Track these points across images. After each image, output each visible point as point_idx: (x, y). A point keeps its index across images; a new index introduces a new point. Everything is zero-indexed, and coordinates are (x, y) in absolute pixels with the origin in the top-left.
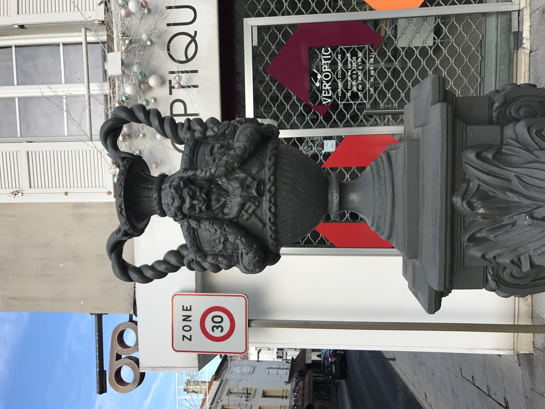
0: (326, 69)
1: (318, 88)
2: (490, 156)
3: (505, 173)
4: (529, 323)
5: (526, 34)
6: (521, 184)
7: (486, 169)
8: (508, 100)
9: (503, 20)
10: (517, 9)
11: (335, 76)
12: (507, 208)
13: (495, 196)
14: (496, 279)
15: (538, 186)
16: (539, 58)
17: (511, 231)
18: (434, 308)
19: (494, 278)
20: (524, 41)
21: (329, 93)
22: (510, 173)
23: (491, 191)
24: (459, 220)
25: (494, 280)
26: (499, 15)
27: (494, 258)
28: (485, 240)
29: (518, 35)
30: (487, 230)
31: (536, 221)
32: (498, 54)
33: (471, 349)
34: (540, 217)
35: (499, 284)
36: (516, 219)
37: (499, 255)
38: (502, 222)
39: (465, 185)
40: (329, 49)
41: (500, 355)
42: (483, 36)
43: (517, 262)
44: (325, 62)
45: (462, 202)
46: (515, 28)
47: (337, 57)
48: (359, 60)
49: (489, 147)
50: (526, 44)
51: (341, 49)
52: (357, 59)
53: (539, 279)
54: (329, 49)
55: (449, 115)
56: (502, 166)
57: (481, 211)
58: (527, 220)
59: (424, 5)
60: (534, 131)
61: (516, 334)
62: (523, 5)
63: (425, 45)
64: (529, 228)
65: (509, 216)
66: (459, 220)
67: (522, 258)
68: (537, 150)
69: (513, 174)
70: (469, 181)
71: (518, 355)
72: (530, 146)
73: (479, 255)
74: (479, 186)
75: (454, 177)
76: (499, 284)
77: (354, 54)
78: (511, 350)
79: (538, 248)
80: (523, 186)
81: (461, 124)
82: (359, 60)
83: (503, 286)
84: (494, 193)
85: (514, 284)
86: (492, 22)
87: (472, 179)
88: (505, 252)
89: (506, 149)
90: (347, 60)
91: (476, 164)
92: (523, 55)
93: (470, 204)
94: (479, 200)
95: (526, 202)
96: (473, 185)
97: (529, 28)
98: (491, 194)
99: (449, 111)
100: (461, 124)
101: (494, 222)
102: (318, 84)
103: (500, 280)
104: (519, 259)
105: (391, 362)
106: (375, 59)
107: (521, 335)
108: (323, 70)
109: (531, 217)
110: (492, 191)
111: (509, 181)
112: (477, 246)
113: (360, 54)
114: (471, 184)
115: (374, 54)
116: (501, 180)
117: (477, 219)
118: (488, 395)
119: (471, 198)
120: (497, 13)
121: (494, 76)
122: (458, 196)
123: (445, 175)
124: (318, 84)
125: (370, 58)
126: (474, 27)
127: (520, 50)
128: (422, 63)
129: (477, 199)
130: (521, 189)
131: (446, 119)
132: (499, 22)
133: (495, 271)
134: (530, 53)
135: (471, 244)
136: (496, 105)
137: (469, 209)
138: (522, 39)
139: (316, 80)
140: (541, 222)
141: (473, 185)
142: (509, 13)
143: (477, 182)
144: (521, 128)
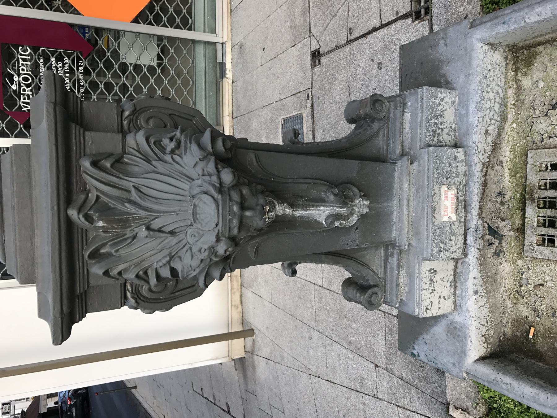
0: (25, 70)
1: (15, 91)
2: (108, 165)
3: (124, 183)
4: (241, 329)
5: (228, 66)
6: (137, 195)
8: (138, 109)
9: (210, 49)
10: (221, 41)
11: (37, 80)
14: (136, 296)
16: (239, 89)
17: (133, 244)
18: (61, 338)
19: (133, 295)
20: (227, 72)
21: (29, 99)
22: (128, 183)
25: (133, 297)
26: (206, 45)
27: (120, 273)
28: (109, 255)
30: (111, 245)
31: (151, 233)
33: (192, 364)
34: (156, 229)
35: (139, 301)
37: (126, 270)
39: (83, 197)
40: (28, 48)
41: (221, 364)
42: (193, 62)
43: (144, 276)
44: (24, 63)
45: (78, 214)
46: (219, 59)
47: (39, 59)
48: (67, 67)
49: (110, 155)
50: (229, 74)
51: (43, 51)
52: (64, 65)
53: (178, 291)
54: (28, 48)
55: (58, 117)
56: (121, 175)
58: (143, 232)
60: (152, 142)
61: (230, 341)
62: (225, 39)
63: (139, 62)
64: (148, 240)
67: (149, 272)
68: (156, 160)
69: (132, 184)
70: (89, 191)
71: (234, 360)
72: (150, 157)
73: (101, 272)
74: (98, 197)
75: (68, 187)
76: (139, 301)
77: (60, 59)
78: (226, 357)
79: (160, 260)
80: (139, 197)
82: (67, 67)
86: (200, 50)
87: (91, 189)
88: (131, 266)
90: (51, 64)
91: (93, 173)
92: (227, 84)
93: (88, 218)
95: (142, 213)
96: (92, 197)
97: (230, 61)
98: (112, 206)
99: (58, 113)
101: (116, 235)
102: (14, 87)
103: (140, 296)
104: (146, 273)
105: (133, 391)
106: (85, 69)
107: (235, 341)
108: (21, 72)
109: (148, 228)
110: (112, 203)
111: (129, 191)
113: (67, 60)
114: (90, 195)
115: (85, 63)
116: (120, 191)
117: (98, 233)
118: (215, 404)
121: (204, 100)
122: (73, 208)
123: (55, 185)
124: (14, 87)
127: (225, 79)
130: (139, 200)
131: (53, 121)
132: (207, 51)
133: (134, 288)
134: (233, 83)
135: (94, 261)
136: (127, 113)
137: (87, 223)
138: (225, 70)
139: (12, 81)
140: (157, 233)
141: (92, 197)
142: (214, 44)
143: (96, 193)
144: (141, 137)
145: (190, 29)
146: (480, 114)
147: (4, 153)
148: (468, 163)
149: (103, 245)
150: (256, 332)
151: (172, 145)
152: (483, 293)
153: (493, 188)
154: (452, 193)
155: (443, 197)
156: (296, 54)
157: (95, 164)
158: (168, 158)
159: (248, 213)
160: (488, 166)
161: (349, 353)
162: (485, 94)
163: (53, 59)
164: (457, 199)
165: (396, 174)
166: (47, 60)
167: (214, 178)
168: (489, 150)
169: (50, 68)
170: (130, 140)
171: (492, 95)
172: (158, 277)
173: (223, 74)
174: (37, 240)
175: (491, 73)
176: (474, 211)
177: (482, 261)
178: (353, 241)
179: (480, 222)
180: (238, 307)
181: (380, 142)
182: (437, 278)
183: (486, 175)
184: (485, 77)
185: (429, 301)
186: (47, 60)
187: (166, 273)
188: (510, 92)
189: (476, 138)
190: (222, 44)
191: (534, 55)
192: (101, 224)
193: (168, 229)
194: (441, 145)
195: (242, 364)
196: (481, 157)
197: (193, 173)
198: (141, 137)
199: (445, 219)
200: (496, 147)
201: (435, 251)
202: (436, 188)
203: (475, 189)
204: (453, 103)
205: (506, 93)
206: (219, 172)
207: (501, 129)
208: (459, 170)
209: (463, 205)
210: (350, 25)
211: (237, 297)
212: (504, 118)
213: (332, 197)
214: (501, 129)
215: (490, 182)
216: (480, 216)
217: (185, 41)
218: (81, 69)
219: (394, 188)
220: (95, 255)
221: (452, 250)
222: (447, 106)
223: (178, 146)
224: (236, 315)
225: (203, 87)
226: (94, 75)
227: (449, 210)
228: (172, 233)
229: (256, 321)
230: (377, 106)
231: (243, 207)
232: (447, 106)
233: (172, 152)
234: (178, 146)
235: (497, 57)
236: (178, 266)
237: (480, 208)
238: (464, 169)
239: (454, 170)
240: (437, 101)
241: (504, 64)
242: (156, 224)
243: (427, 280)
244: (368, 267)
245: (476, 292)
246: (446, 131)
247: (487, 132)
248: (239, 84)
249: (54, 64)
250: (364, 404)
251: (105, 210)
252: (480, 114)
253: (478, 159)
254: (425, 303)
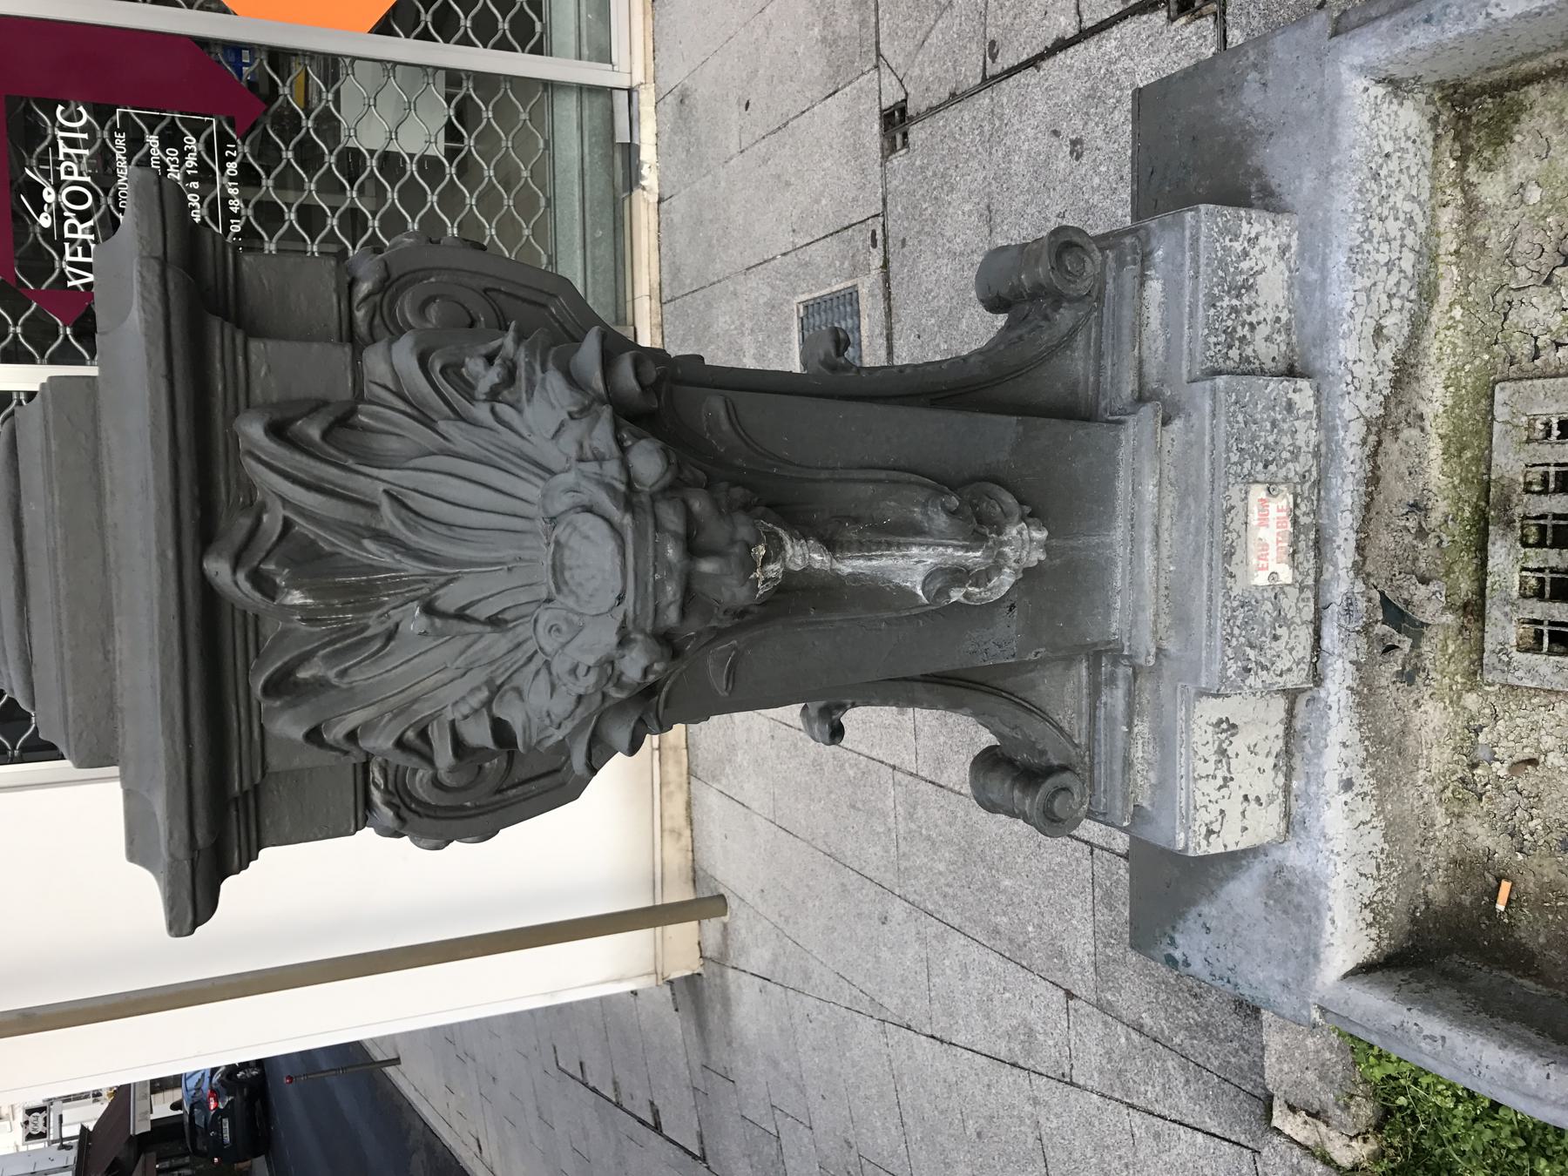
1: (47, 233)
2: (315, 433)
3: (359, 484)
4: (688, 895)
5: (648, 154)
6: (398, 517)
7: (305, 472)
8: (395, 275)
9: (595, 105)
10: (626, 85)
11: (110, 201)
12: (366, 592)
13: (332, 554)
14: (396, 801)
15: (446, 520)
16: (677, 218)
17: (387, 654)
18: (190, 917)
19: (388, 797)
20: (645, 171)
21: (87, 253)
22: (373, 483)
23: (325, 540)
24: (239, 634)
25: (389, 804)
26: (585, 95)
27: (352, 736)
28: (320, 685)
29: (630, 151)
30: (325, 657)
31: (438, 622)
32: (587, 195)
33: (552, 993)
34: (452, 610)
35: (405, 813)
36: (396, 619)
37: (368, 726)
38: (363, 630)
39: (246, 522)
40: (81, 109)
41: (634, 993)
42: (546, 143)
43: (418, 743)
44: (72, 151)
45: (234, 571)
46: (622, 136)
47: (113, 139)
48: (191, 161)
49: (315, 407)
51: (124, 116)
52: (183, 155)
53: (514, 786)
54: (81, 109)
55: (172, 298)
56: (350, 462)
57: (296, 598)
58: (414, 621)
59: (383, 28)
60: (438, 367)
61: (659, 929)
62: (638, 78)
63: (394, 147)
64: (429, 643)
65: (380, 612)
66: (239, 634)
67: (434, 732)
68: (448, 418)
69: (381, 487)
70: (263, 508)
71: (671, 982)
72: (432, 408)
73: (298, 733)
74: (287, 524)
75: (204, 496)
76: (405, 813)
77: (171, 139)
78: (649, 974)
79: (463, 698)
80: (404, 522)
81: (227, 332)
82: (191, 161)
83: (416, 818)
84: (333, 544)
85: (445, 808)
86: (567, 110)
87: (269, 504)
88: (382, 716)
89: (367, 414)
90: (148, 155)
91: (274, 456)
92: (643, 205)
93: (260, 581)
94: (285, 567)
95: (412, 567)
96: (272, 523)
97: (653, 139)
98: (327, 548)
99: (171, 286)
100: (227, 332)
101: (341, 629)
102: (45, 221)
103: (407, 800)
104: (423, 734)
105: (390, 1070)
106: (244, 167)
107: (672, 930)
108: (63, 177)
109: (429, 610)
110: (328, 540)
111: (373, 507)
112: (295, 706)
113: (191, 142)
114: (265, 518)
115: (242, 150)
116: (350, 507)
117: (292, 626)
118: (618, 1105)
119: (262, 561)
120: (581, 88)
121: (579, 253)
122: (219, 555)
123: (167, 489)
124: (45, 221)
125: (223, 161)
126: (524, 116)
127: (637, 193)
128: (389, 195)
129: (277, 564)
130: (402, 532)
131: (160, 308)
132: (586, 113)
133: (391, 777)
134: (660, 201)
135: (278, 703)
136: (364, 288)
137: (258, 596)
138: (639, 167)
139: (39, 205)
140: (454, 622)
141: (272, 523)
142: (607, 92)
143: (281, 512)
144: (404, 354)
145: (538, 50)
146: (1360, 282)
147: (20, 403)
148: (1324, 420)
149: (304, 658)
150: (733, 903)
151: (493, 376)
152: (1369, 786)
153: (1397, 491)
154: (1280, 506)
155: (1254, 519)
156: (838, 117)
157: (277, 430)
158: (482, 412)
159: (707, 566)
160: (1381, 429)
161: (994, 960)
162: (1374, 223)
163: (153, 140)
164: (1295, 522)
165: (1124, 453)
166: (135, 142)
167: (612, 469)
168: (1384, 382)
169: (145, 162)
170: (375, 362)
171: (1393, 227)
172: (459, 746)
173: (632, 178)
174: (122, 645)
175: (1393, 164)
176: (1344, 557)
177: (1365, 697)
178: (1000, 642)
179: (1360, 587)
180: (680, 835)
181: (1078, 363)
182: (1239, 744)
183: (1375, 454)
184: (1376, 176)
185: (1214, 810)
186: (135, 142)
187: (479, 734)
188: (1446, 217)
189: (1348, 348)
190: (630, 91)
191: (1515, 112)
192: (296, 598)
193: (483, 611)
194: (1249, 369)
195: (691, 993)
196: (1363, 404)
197: (556, 454)
198: (404, 354)
199: (1261, 579)
200: (1404, 373)
201: (1233, 668)
202: (1235, 493)
203: (1346, 493)
204: (1283, 250)
205: (1434, 220)
206: (623, 450)
207: (1418, 325)
208: (1301, 439)
209: (1311, 539)
210: (992, 33)
211: (677, 807)
212: (1428, 293)
213: (941, 521)
214: (1418, 325)
215: (1387, 474)
216: (1358, 568)
217: (524, 85)
218: (232, 167)
219: (1115, 493)
220: (283, 685)
221: (1281, 665)
222: (1266, 260)
223: (510, 378)
224: (675, 857)
225: (578, 216)
226: (268, 183)
227: (1273, 553)
228: (495, 622)
229: (733, 870)
230: (1069, 260)
231: (693, 548)
232: (1266, 260)
233: (494, 395)
234: (510, 378)
235: (1410, 117)
236: (514, 715)
237: (1360, 549)
238: (1314, 437)
239: (1286, 440)
240: (1238, 246)
241: (1429, 138)
242: (450, 599)
243: (1209, 752)
244: (1044, 716)
245: (1348, 785)
246: (1263, 330)
247: (1378, 331)
248: (678, 204)
249: (156, 152)
250: (1035, 1102)
251: (308, 561)
252: (1360, 282)
253: (1354, 409)
254: (1203, 817)
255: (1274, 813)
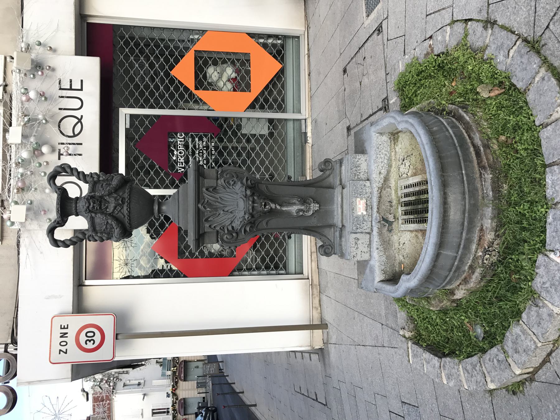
0: (181, 148)
1: (175, 161)
5: (309, 134)
12: (216, 209)
20: (308, 139)
22: (217, 196)
27: (215, 227)
28: (211, 220)
29: (306, 133)
33: (283, 348)
46: (303, 131)
48: (204, 143)
50: (310, 140)
52: (203, 142)
57: (208, 209)
58: (222, 212)
62: (307, 116)
77: (201, 139)
82: (204, 143)
86: (290, 125)
93: (204, 207)
95: (222, 206)
96: (206, 201)
102: (174, 158)
104: (223, 228)
105: (253, 408)
109: (223, 211)
113: (205, 139)
118: (308, 397)
120: (294, 120)
124: (174, 158)
125: (211, 142)
139: (173, 155)
141: (206, 201)
142: (300, 120)
145: (283, 112)
146: (376, 165)
147: (167, 199)
148: (371, 187)
149: (209, 217)
150: (329, 325)
151: (233, 183)
152: (382, 249)
153: (385, 199)
154: (363, 202)
155: (358, 203)
156: (341, 128)
157: (207, 189)
158: (231, 187)
159: (256, 205)
160: (381, 189)
161: (371, 321)
162: (378, 155)
163: (197, 139)
164: (366, 204)
165: (336, 194)
166: (193, 140)
167: (244, 193)
168: (382, 181)
169: (195, 158)
170: (219, 181)
171: (382, 156)
172: (228, 230)
173: (306, 141)
174: (189, 215)
175: (382, 146)
176: (375, 210)
177: (380, 234)
178: (314, 222)
179: (378, 215)
180: (317, 309)
181: (331, 179)
182: (360, 242)
183: (380, 193)
184: (378, 148)
185: (355, 253)
186: (193, 140)
187: (230, 228)
188: (393, 154)
189: (374, 176)
190: (305, 119)
191: (398, 137)
192: (208, 209)
193: (230, 211)
194: (359, 180)
195: (321, 353)
196: (377, 185)
197: (238, 192)
198: (222, 180)
199: (360, 213)
200: (386, 179)
201: (354, 228)
202: (354, 199)
203: (375, 200)
204: (366, 160)
205: (391, 154)
206: (246, 191)
207: (388, 172)
208: (367, 191)
209: (368, 207)
210: (362, 112)
211: (316, 301)
212: (390, 166)
213: (297, 202)
214: (388, 172)
215: (383, 196)
216: (378, 212)
217: (280, 120)
218: (213, 144)
219: (334, 201)
220: (206, 220)
221: (364, 228)
222: (362, 162)
223: (235, 183)
224: (316, 315)
225: (293, 150)
226: (221, 147)
227: (362, 209)
228: (231, 212)
229: (329, 318)
230: (327, 164)
231: (253, 202)
232: (362, 162)
233: (233, 185)
234: (235, 183)
235: (385, 138)
236: (234, 225)
237: (378, 208)
238: (370, 190)
239: (364, 191)
240: (356, 160)
241: (389, 141)
242: (226, 209)
243: (354, 243)
244: (325, 236)
245: (378, 249)
246: (362, 173)
247: (380, 173)
248: (315, 146)
249: (197, 142)
250: (379, 354)
251: (210, 205)
252: (376, 165)
253: (376, 186)
254: (352, 254)
255: (368, 255)
